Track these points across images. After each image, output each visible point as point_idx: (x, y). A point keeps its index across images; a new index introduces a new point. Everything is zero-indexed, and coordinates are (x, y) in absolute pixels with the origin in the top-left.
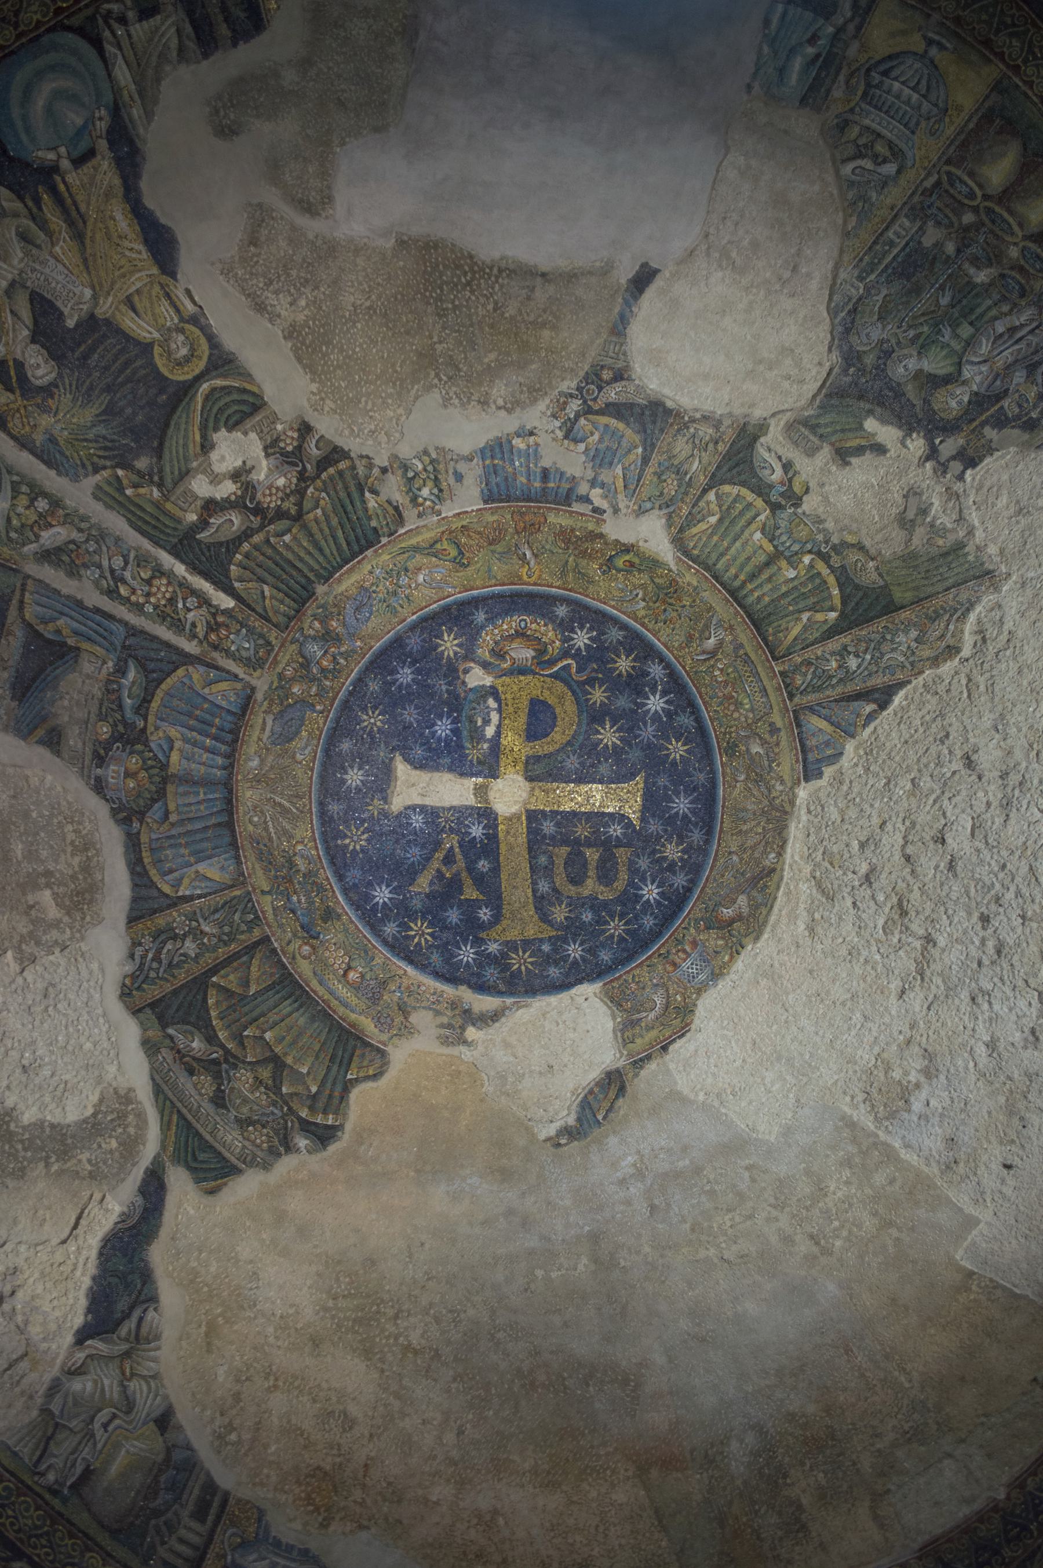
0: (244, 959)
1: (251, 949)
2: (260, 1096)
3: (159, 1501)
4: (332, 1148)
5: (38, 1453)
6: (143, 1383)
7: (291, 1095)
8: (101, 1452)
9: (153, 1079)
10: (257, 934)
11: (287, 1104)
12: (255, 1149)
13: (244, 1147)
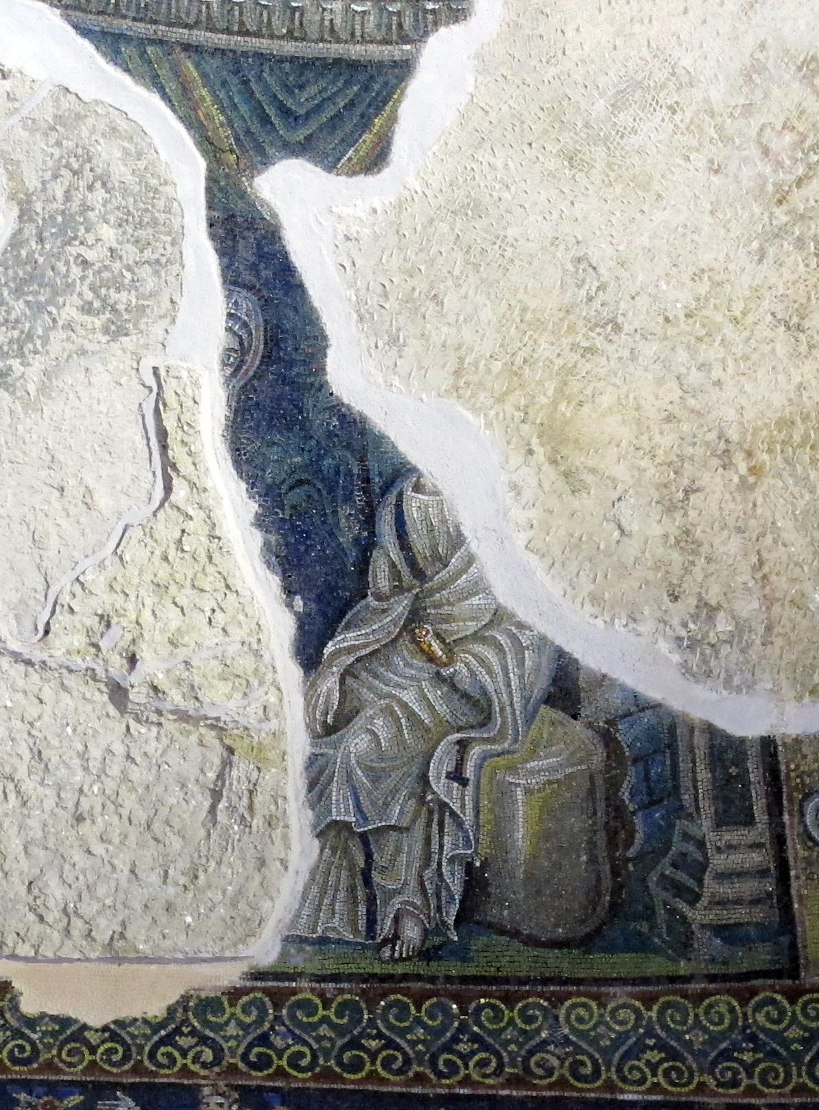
3: (639, 837)
5: (362, 910)
6: (478, 648)
8: (477, 826)
9: (84, 32)
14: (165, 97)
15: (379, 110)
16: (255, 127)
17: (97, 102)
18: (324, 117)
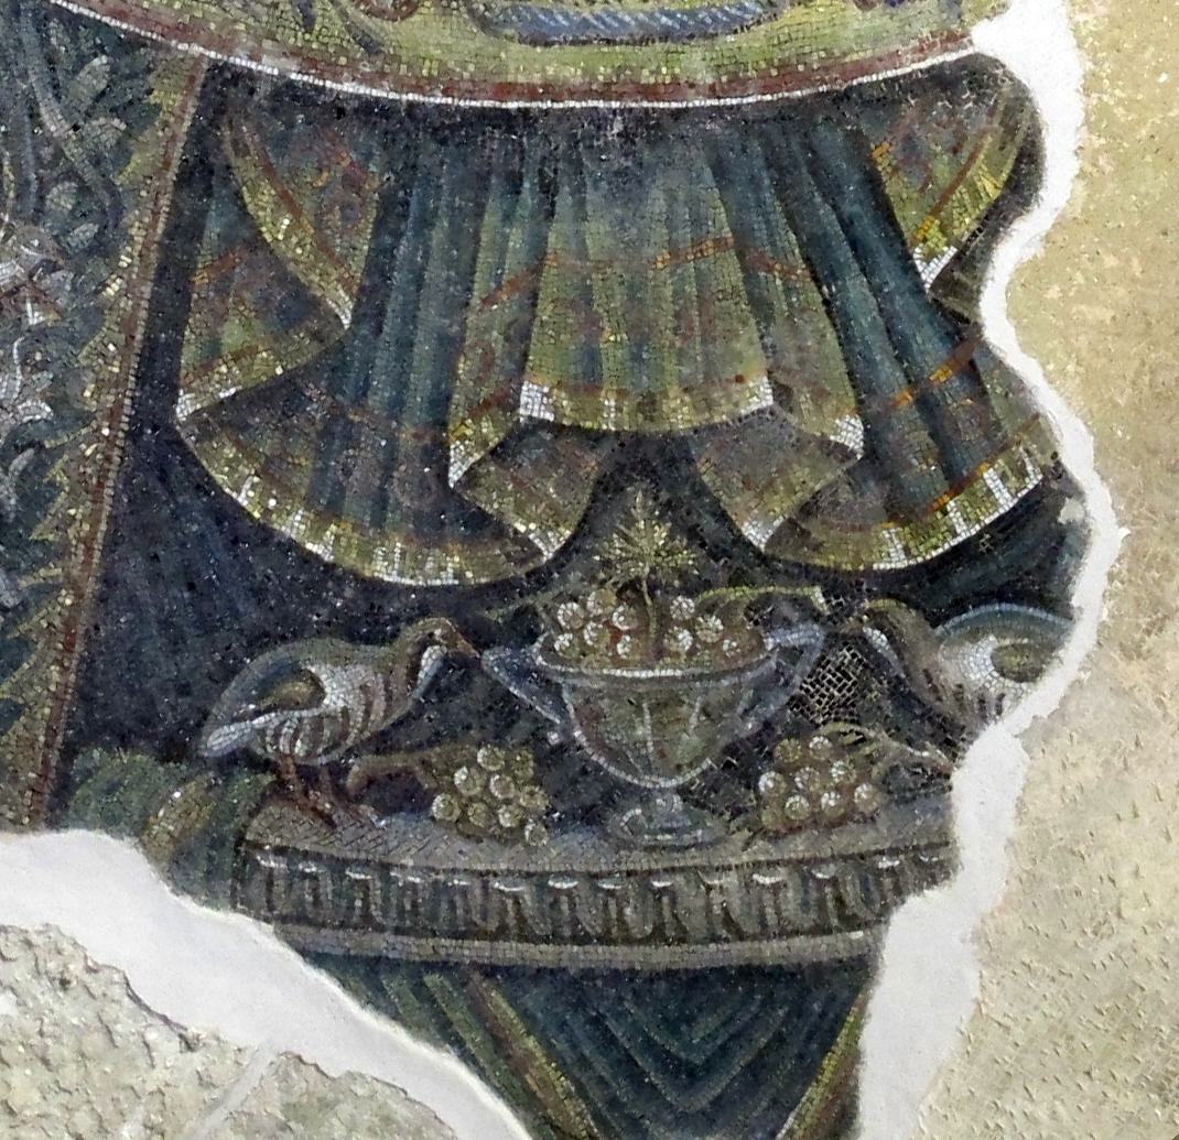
0: (213, 229)
1: (201, 173)
2: (699, 632)
4: (1090, 587)
7: (794, 529)
9: (317, 958)
10: (176, 104)
11: (809, 574)
12: (840, 841)
13: (802, 868)
14: (467, 1058)
15: (826, 1048)
16: (622, 1090)
17: (352, 1076)
18: (741, 1060)
